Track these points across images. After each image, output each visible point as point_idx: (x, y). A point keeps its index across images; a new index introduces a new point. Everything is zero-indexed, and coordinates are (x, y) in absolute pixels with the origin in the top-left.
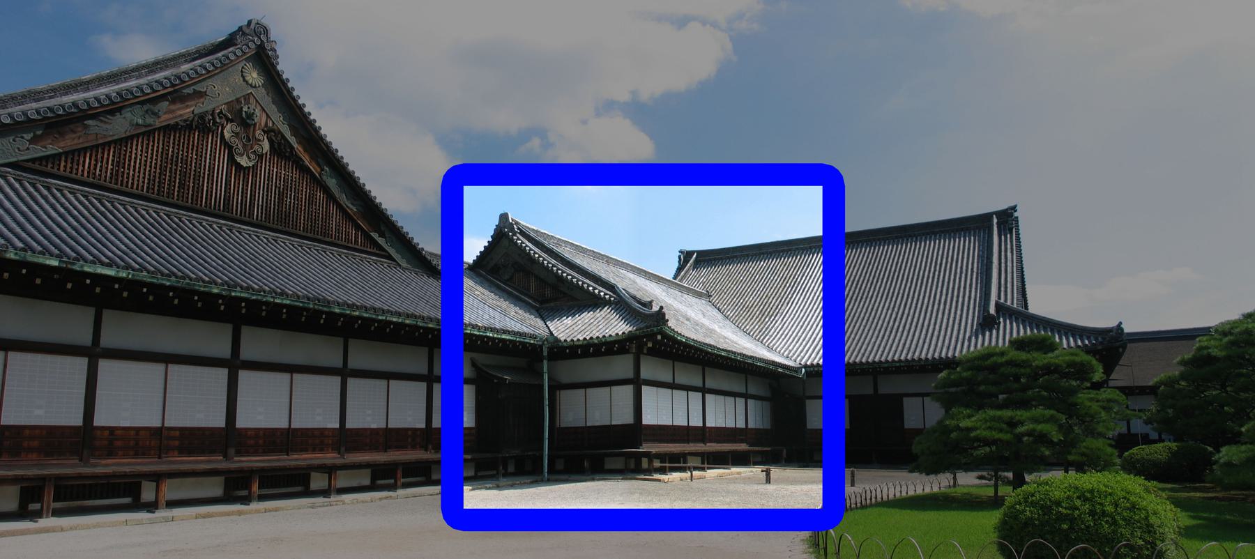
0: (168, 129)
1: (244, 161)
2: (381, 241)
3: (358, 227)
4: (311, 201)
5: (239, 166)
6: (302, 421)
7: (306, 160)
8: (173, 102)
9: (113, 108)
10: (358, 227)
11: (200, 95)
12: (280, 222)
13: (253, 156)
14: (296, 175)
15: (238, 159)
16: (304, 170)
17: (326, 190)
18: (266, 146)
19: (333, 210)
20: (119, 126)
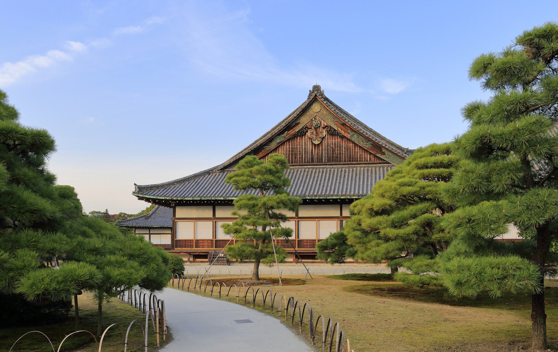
0: (289, 140)
1: (316, 142)
2: (382, 157)
3: (371, 154)
4: (347, 149)
5: (315, 145)
6: (200, 237)
7: (343, 132)
8: (289, 130)
9: (271, 140)
10: (371, 154)
11: (298, 124)
12: (334, 159)
13: (319, 139)
14: (339, 140)
15: (314, 142)
16: (343, 137)
17: (353, 143)
18: (325, 133)
19: (357, 149)
20: (273, 145)
